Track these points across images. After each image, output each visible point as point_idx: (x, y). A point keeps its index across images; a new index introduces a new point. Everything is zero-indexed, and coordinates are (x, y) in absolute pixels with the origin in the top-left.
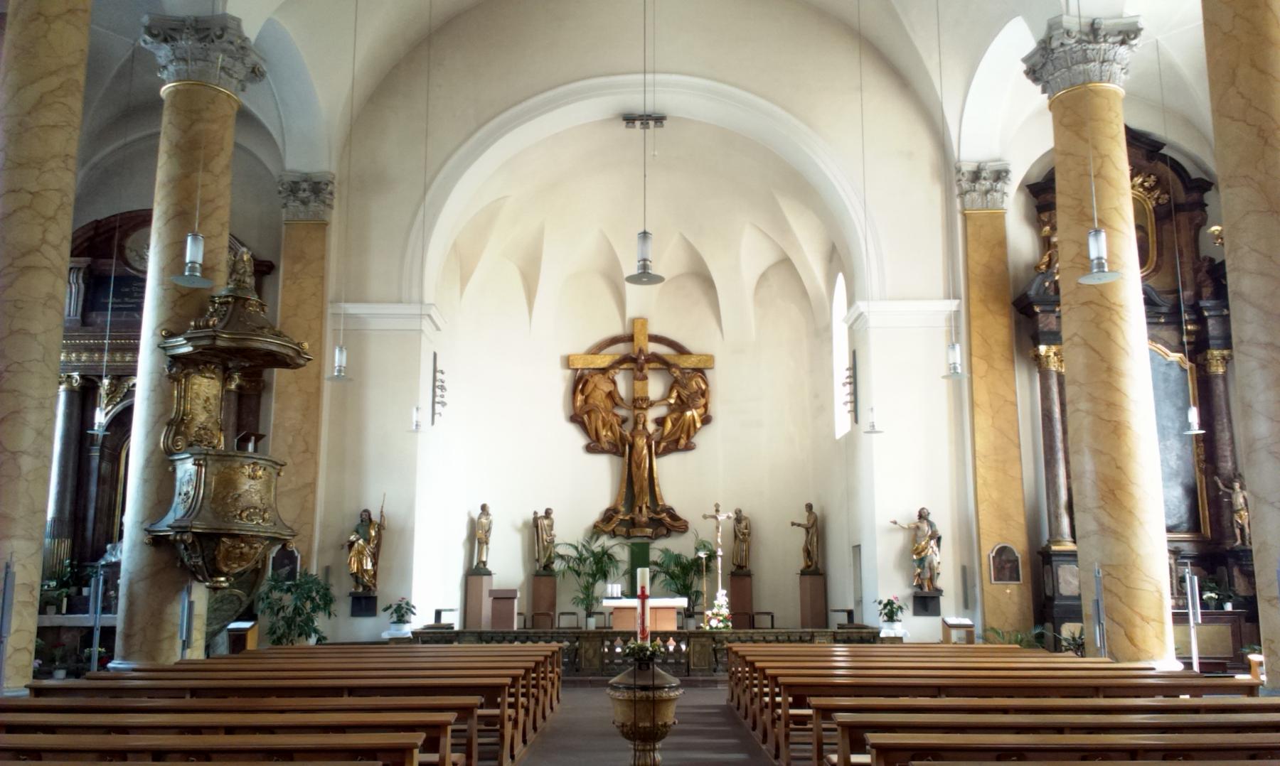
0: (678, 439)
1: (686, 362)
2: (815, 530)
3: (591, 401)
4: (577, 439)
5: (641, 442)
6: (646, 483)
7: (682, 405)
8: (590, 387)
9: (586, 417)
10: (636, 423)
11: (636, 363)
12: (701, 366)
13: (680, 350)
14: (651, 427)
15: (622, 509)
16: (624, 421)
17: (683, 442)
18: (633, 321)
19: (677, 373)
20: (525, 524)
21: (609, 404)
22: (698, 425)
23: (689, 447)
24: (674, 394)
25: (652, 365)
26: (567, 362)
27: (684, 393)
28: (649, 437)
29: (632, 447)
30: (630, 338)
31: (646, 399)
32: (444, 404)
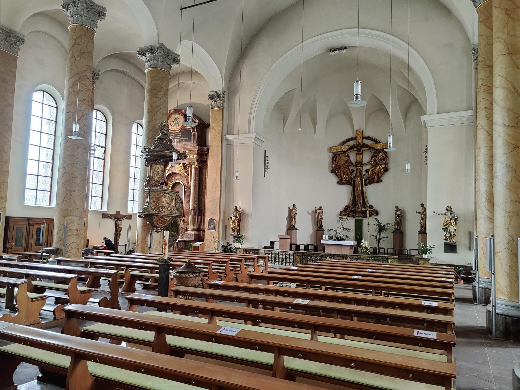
0: (376, 178)
1: (378, 146)
3: (339, 164)
4: (334, 179)
5: (358, 179)
6: (360, 196)
7: (376, 165)
8: (338, 159)
9: (336, 171)
14: (364, 173)
16: (353, 171)
17: (376, 179)
20: (313, 212)
23: (379, 181)
24: (373, 160)
25: (364, 149)
26: (330, 150)
27: (377, 159)
29: (355, 181)
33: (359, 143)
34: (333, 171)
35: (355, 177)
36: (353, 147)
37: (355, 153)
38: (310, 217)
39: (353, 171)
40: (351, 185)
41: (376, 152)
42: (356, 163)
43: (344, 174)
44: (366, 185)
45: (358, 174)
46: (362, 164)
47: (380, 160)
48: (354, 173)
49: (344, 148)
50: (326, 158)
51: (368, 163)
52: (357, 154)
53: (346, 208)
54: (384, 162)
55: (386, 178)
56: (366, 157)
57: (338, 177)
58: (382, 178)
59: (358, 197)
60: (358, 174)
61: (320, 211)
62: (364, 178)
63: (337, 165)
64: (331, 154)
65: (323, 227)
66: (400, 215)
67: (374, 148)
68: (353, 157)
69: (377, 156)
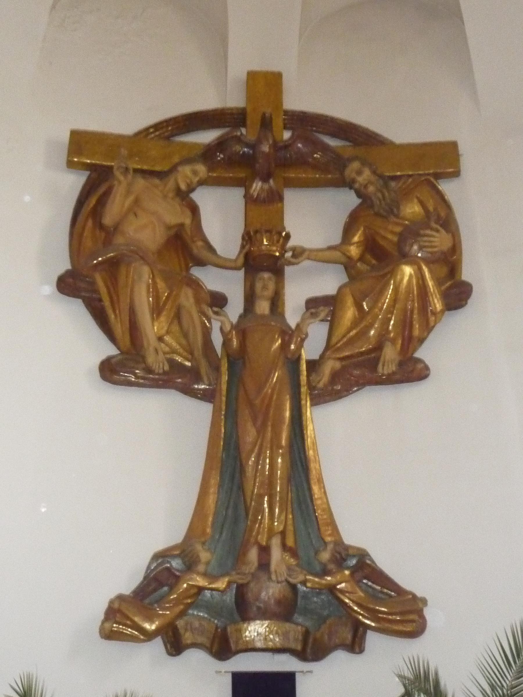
16: (219, 301)
17: (390, 354)
23: (411, 371)
28: (287, 334)
43: (157, 310)
44: (321, 397)
45: (263, 307)
52: (249, 199)
53: (159, 580)
56: (313, 218)
60: (263, 307)
68: (221, 216)
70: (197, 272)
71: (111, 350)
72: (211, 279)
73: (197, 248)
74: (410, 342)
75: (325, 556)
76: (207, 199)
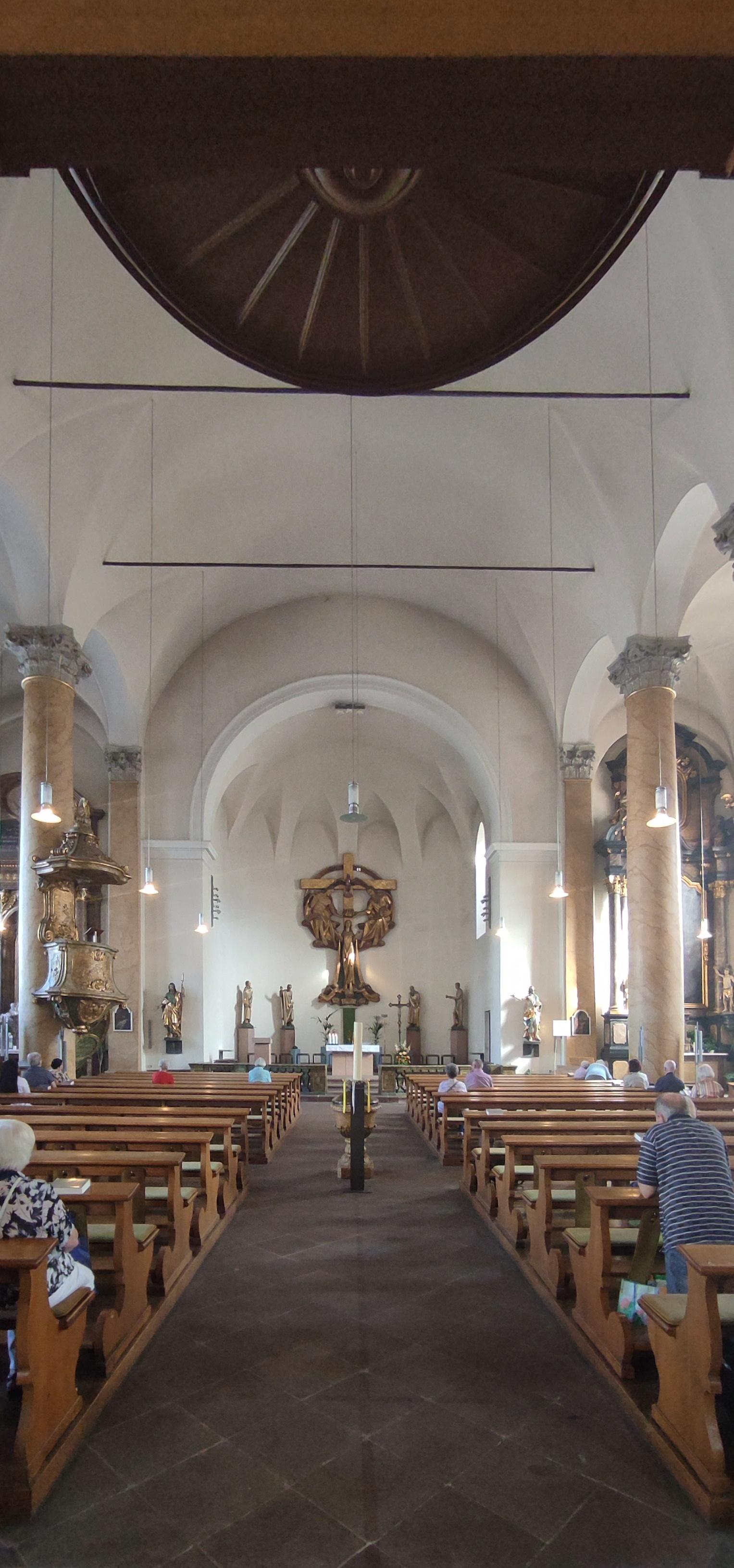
1: (379, 885)
2: (462, 1000)
3: (315, 911)
4: (306, 937)
7: (376, 916)
9: (312, 923)
10: (345, 927)
11: (347, 885)
12: (388, 888)
13: (375, 877)
14: (355, 930)
15: (337, 986)
17: (376, 941)
18: (344, 855)
19: (373, 893)
20: (275, 995)
21: (327, 914)
22: (386, 929)
23: (381, 944)
24: (370, 908)
25: (355, 887)
26: (300, 884)
27: (377, 907)
28: (354, 936)
30: (341, 867)
31: (352, 910)
32: (219, 912)
33: (348, 876)
34: (305, 923)
35: (343, 935)
36: (339, 882)
37: (341, 893)
38: (270, 1005)
39: (338, 925)
40: (337, 949)
41: (376, 895)
42: (345, 911)
43: (324, 928)
45: (348, 930)
46: (354, 914)
47: (383, 909)
48: (340, 929)
49: (323, 883)
50: (293, 899)
51: (363, 912)
52: (344, 896)
54: (389, 913)
55: (391, 939)
57: (314, 935)
58: (384, 939)
59: (349, 971)
60: (348, 930)
61: (288, 993)
62: (358, 936)
63: (312, 911)
64: (300, 892)
65: (293, 1023)
66: (416, 999)
67: (372, 887)
69: (378, 902)
70: (333, 918)
71: (314, 939)
72: (336, 919)
73: (333, 911)
74: (380, 937)
75: (360, 986)
76: (334, 896)
